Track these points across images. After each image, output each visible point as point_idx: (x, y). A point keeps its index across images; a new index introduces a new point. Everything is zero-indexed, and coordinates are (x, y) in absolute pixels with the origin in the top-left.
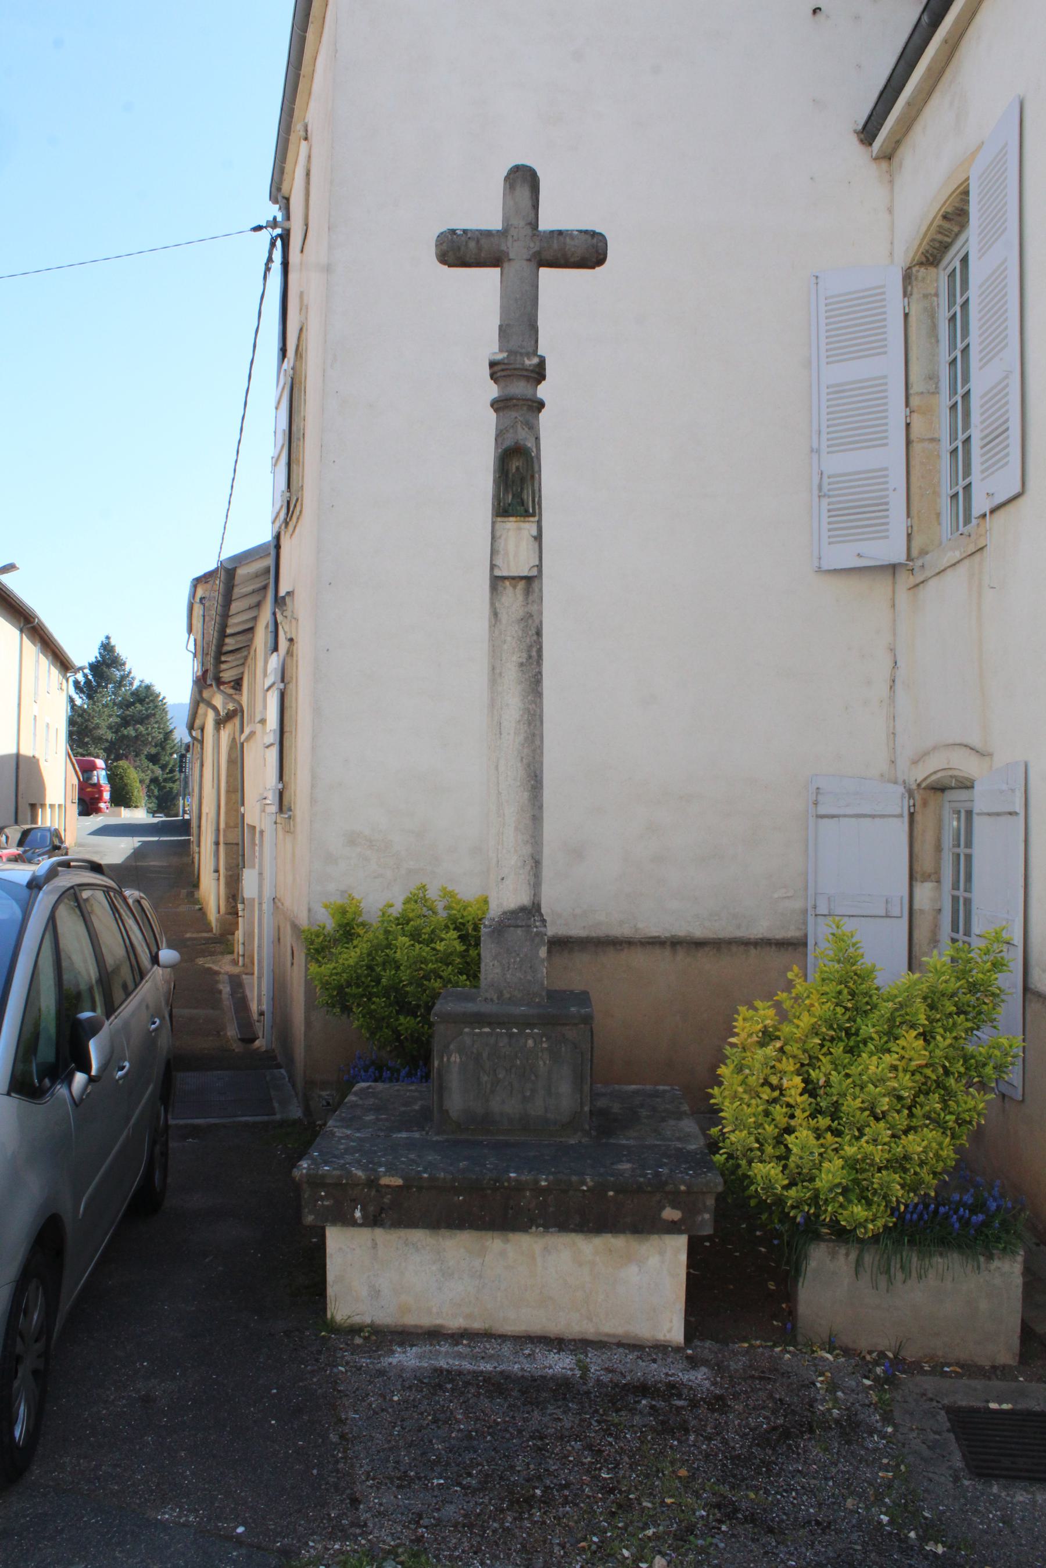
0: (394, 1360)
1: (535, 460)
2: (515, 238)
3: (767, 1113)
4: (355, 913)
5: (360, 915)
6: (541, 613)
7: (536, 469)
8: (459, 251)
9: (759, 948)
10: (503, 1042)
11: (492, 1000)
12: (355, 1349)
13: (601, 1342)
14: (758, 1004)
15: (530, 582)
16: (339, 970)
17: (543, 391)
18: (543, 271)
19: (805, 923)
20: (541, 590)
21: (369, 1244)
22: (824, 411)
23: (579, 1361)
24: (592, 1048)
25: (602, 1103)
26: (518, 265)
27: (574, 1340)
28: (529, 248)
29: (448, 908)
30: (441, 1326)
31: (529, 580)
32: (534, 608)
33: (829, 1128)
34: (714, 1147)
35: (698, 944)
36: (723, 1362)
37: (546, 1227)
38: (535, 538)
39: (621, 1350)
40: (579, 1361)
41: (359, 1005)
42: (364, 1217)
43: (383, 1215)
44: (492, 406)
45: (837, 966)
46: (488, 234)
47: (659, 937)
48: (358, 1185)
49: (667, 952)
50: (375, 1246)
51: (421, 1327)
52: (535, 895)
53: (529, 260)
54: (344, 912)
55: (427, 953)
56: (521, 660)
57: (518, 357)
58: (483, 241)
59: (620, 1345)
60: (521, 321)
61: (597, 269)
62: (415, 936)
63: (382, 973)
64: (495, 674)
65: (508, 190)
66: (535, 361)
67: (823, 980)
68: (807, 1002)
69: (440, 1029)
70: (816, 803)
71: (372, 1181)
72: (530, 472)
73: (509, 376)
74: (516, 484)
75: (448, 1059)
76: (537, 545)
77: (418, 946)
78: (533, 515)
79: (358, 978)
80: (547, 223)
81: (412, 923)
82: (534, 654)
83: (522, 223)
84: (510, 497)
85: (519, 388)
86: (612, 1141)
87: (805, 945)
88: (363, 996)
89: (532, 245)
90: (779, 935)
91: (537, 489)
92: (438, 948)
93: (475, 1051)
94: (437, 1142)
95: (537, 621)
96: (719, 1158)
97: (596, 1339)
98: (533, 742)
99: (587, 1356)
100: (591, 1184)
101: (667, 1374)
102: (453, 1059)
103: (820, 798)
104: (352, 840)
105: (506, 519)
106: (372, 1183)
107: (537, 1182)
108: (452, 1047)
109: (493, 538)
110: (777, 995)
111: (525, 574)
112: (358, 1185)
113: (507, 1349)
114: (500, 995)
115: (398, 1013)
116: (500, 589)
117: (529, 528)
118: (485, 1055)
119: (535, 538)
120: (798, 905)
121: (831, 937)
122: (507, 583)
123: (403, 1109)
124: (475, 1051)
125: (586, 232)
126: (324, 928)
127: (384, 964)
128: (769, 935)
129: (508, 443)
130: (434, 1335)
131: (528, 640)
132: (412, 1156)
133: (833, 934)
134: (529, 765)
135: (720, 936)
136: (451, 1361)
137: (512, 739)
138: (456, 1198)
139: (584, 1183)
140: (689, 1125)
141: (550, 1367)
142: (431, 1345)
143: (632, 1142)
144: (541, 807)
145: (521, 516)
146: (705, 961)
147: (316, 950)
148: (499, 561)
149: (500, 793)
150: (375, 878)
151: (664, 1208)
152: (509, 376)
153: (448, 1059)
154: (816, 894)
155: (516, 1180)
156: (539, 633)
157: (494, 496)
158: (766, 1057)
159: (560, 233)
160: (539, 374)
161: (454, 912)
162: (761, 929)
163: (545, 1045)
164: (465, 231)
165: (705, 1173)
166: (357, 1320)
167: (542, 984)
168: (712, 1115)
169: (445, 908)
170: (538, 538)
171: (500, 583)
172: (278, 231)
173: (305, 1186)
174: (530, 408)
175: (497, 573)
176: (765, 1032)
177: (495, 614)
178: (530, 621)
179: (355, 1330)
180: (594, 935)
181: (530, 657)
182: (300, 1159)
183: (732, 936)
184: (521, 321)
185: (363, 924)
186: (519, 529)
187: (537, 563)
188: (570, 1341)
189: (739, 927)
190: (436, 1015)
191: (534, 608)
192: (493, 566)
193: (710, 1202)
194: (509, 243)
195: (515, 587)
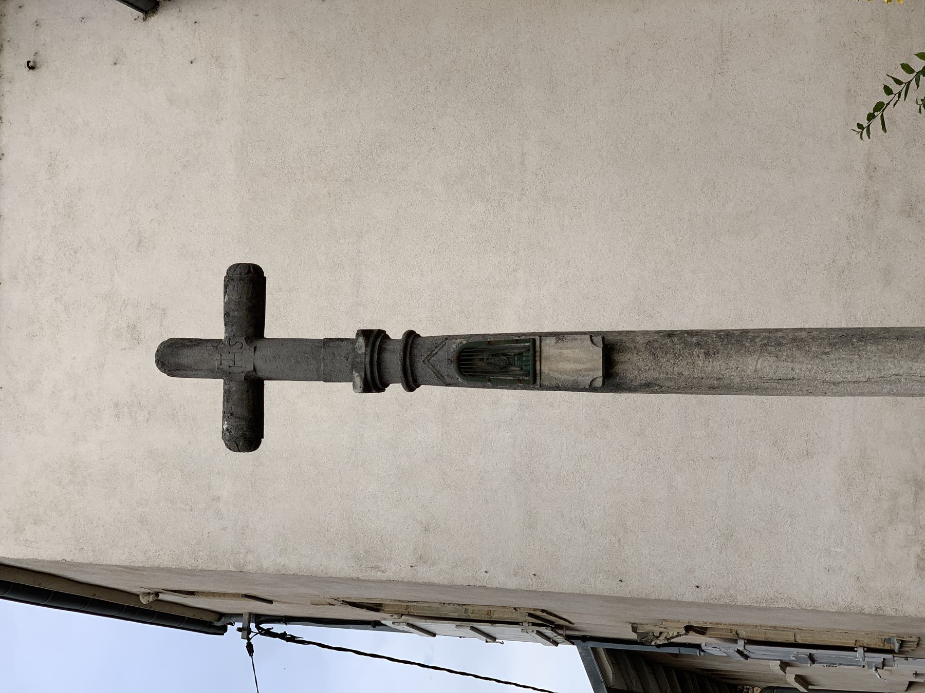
1: (471, 340)
2: (231, 364)
6: (646, 333)
7: (481, 339)
8: (246, 428)
17: (396, 333)
18: (268, 334)
32: (640, 340)
46: (227, 394)
56: (702, 356)
66: (361, 340)
78: (534, 340)
80: (216, 330)
82: (694, 339)
84: (513, 368)
98: (802, 340)
109: (558, 388)
125: (226, 287)
129: (452, 370)
149: (869, 380)
156: (670, 334)
159: (227, 314)
160: (375, 338)
177: (648, 387)
178: (656, 345)
181: (698, 344)
186: (547, 358)
191: (640, 340)
192: (592, 388)
194: (236, 370)
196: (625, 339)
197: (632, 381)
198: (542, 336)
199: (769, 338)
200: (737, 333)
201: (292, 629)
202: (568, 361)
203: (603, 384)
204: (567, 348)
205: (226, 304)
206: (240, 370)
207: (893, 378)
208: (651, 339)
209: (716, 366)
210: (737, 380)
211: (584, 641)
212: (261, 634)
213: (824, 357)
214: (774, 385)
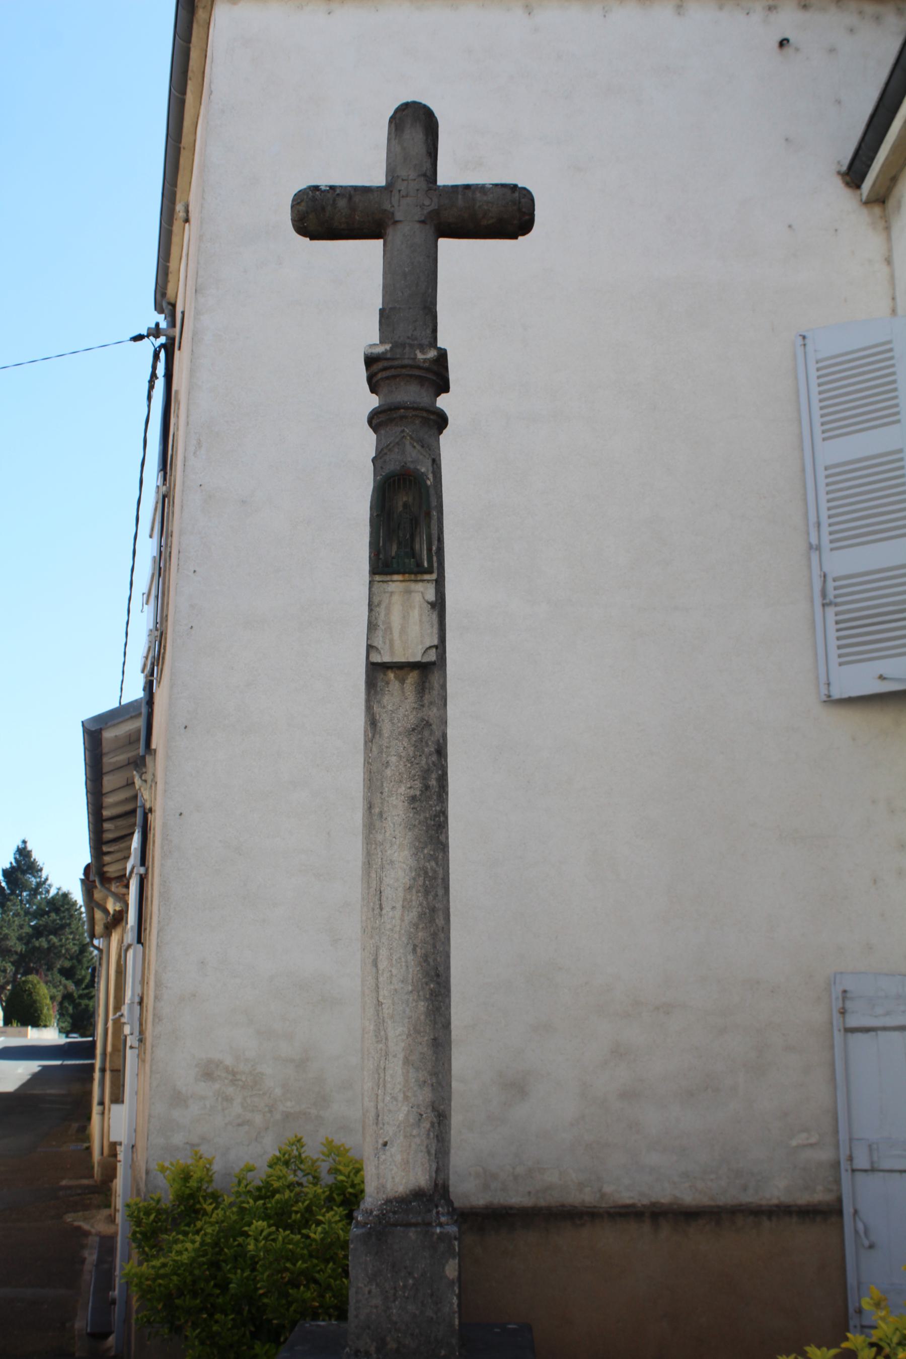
1: (432, 491)
4: (201, 1180)
5: (211, 1181)
7: (434, 503)
8: (324, 215)
15: (428, 672)
16: (167, 1270)
18: (443, 242)
19: (838, 1181)
20: (444, 687)
22: (823, 497)
26: (407, 230)
28: (422, 206)
29: (334, 1171)
32: (433, 713)
38: (433, 605)
41: (195, 1326)
44: (370, 422)
47: (633, 1206)
52: (437, 1171)
53: (423, 222)
55: (297, 1244)
56: (412, 792)
57: (407, 349)
58: (357, 199)
60: (411, 305)
61: (520, 238)
62: (280, 1218)
63: (231, 1276)
64: (373, 815)
65: (393, 135)
66: (432, 354)
70: (843, 1012)
73: (394, 377)
74: (406, 527)
76: (435, 617)
77: (282, 1234)
78: (431, 572)
79: (194, 1282)
80: (448, 174)
81: (277, 1196)
82: (433, 782)
83: (413, 175)
85: (410, 394)
87: (840, 1212)
89: (427, 202)
90: (803, 1199)
91: (435, 532)
92: (312, 1235)
95: (438, 734)
98: (432, 920)
103: (849, 1005)
104: (208, 1072)
105: (388, 578)
110: (847, 1339)
111: (418, 658)
119: (433, 605)
120: (825, 1155)
122: (391, 675)
126: (158, 1201)
127: (235, 1258)
128: (786, 1199)
134: (426, 958)
135: (721, 1203)
137: (398, 918)
144: (447, 1026)
145: (410, 573)
148: (378, 642)
149: (380, 1004)
150: (239, 1125)
152: (394, 377)
154: (851, 1140)
156: (441, 751)
157: (370, 543)
159: (467, 187)
161: (341, 1178)
164: (332, 188)
169: (331, 1171)
170: (439, 605)
171: (381, 676)
172: (162, 340)
174: (425, 422)
175: (376, 658)
177: (373, 723)
178: (426, 733)
180: (542, 1203)
181: (427, 787)
184: (411, 305)
185: (215, 1197)
186: (409, 592)
187: (436, 642)
189: (745, 1188)
191: (434, 712)
192: (370, 648)
195: (402, 681)
196: (435, 693)
197: (379, 702)
198: (440, 584)
199: (435, 878)
200: (442, 838)
201: (160, 384)
202: (404, 617)
204: (421, 615)
205: (481, 188)
206: (396, 205)
207: (382, 1033)
208: (434, 727)
209: (397, 810)
210: (380, 838)
212: (155, 350)
213: (410, 947)
214: (374, 884)
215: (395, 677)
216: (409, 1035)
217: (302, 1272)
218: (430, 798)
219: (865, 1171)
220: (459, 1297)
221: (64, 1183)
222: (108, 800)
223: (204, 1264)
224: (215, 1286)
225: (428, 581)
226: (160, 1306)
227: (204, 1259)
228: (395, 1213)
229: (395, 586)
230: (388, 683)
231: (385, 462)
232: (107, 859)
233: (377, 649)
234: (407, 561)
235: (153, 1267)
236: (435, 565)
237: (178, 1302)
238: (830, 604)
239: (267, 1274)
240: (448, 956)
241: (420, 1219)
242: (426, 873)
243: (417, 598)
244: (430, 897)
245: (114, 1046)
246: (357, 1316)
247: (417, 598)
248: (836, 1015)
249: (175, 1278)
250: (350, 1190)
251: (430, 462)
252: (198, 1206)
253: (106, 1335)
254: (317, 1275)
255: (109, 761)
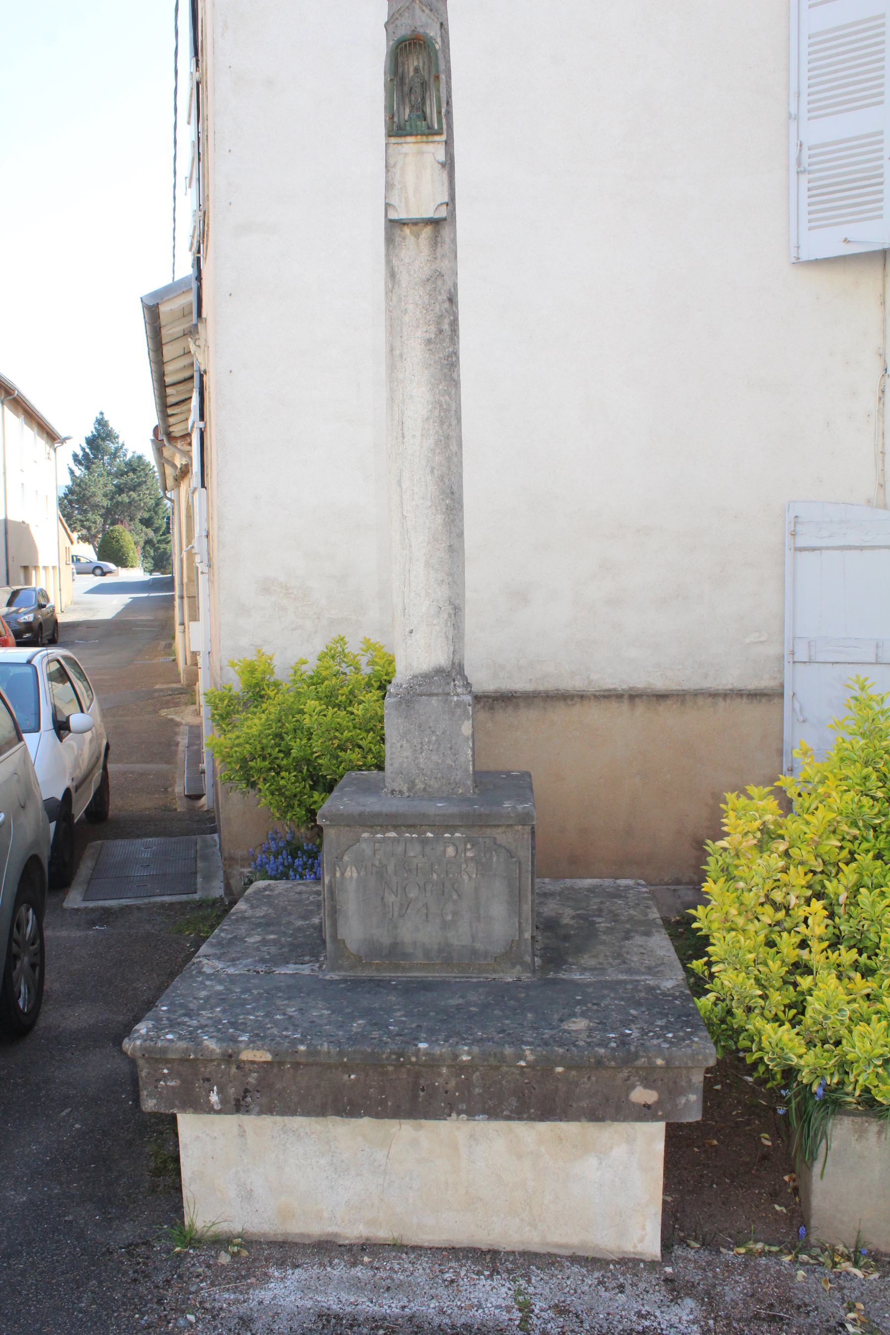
0: (265, 1295)
1: (440, 55)
3: (771, 944)
4: (264, 672)
7: (442, 67)
9: (728, 701)
10: (414, 851)
11: (401, 792)
12: (219, 1276)
13: (549, 1255)
14: (752, 790)
16: (241, 740)
19: (781, 671)
20: (454, 241)
21: (235, 1130)
23: (519, 1292)
24: (533, 855)
25: (550, 908)
27: (513, 1252)
30: (336, 1235)
31: (435, 223)
32: (444, 265)
33: (856, 966)
34: (699, 985)
35: (661, 697)
36: (714, 1286)
37: (471, 1114)
38: (443, 165)
39: (575, 1269)
40: (519, 1292)
42: (223, 1101)
43: (249, 1099)
45: (862, 742)
47: (615, 690)
48: (212, 1061)
49: (625, 706)
50: (242, 1134)
51: (309, 1236)
52: (454, 651)
54: (253, 671)
55: (343, 718)
56: (428, 336)
59: (575, 1259)
62: (330, 699)
63: (292, 743)
64: (394, 357)
67: (842, 760)
68: (821, 790)
69: (330, 835)
70: (794, 534)
71: (230, 1056)
72: (433, 72)
75: (343, 874)
77: (331, 710)
78: (439, 133)
79: (263, 749)
81: (326, 682)
82: (446, 327)
86: (561, 975)
87: (781, 695)
88: (270, 769)
90: (752, 684)
92: (355, 711)
93: (377, 863)
94: (332, 982)
95: (450, 284)
96: (705, 1003)
97: (542, 1250)
98: (447, 446)
99: (529, 1282)
100: (531, 1057)
101: (639, 1315)
102: (348, 874)
103: (799, 528)
104: (266, 587)
105: (402, 140)
106: (229, 1058)
107: (456, 1056)
108: (346, 858)
110: (779, 780)
111: (430, 214)
112: (212, 1061)
113: (422, 1271)
114: (412, 785)
115: (312, 788)
116: (397, 239)
117: (435, 151)
118: (391, 868)
119: (443, 165)
121: (853, 703)
122: (407, 231)
123: (300, 923)
124: (377, 863)
126: (230, 690)
127: (295, 730)
128: (739, 685)
129: (403, 31)
130: (326, 1248)
131: (437, 309)
132: (291, 1011)
133: (856, 699)
134: (442, 478)
135: (686, 688)
136: (344, 1296)
137: (419, 444)
138: (346, 1077)
139: (522, 1057)
140: (661, 945)
141: (480, 1306)
142: (322, 1265)
143: (587, 977)
144: (461, 535)
145: (423, 135)
146: (668, 717)
147: (221, 716)
148: (394, 201)
150: (293, 629)
151: (633, 1087)
153: (343, 874)
154: (794, 638)
155: (427, 1054)
156: (452, 300)
157: (385, 107)
158: (768, 868)
162: (730, 680)
163: (470, 854)
165: (689, 1036)
166: (224, 1227)
167: (467, 770)
168: (692, 943)
169: (368, 664)
170: (449, 165)
171: (397, 231)
173: (141, 1062)
175: (393, 216)
176: (764, 829)
177: (392, 275)
178: (439, 283)
179: (221, 1242)
182: (137, 1020)
183: (698, 687)
185: (277, 685)
186: (421, 153)
187: (446, 199)
188: (508, 1253)
190: (323, 816)
192: (387, 205)
193: (698, 1078)
195: (417, 236)
196: (446, 246)
198: (449, 144)
199: (449, 411)
200: (455, 376)
203: (391, 221)
207: (407, 541)
208: (446, 277)
209: (415, 352)
210: (401, 376)
211: (196, 279)
213: (428, 470)
215: (411, 233)
216: (429, 543)
217: (347, 740)
218: (443, 340)
219: (805, 662)
220: (473, 750)
221: (157, 687)
222: (168, 368)
223: (269, 735)
224: (280, 751)
225: (439, 142)
226: (238, 768)
227: (270, 732)
228: (420, 685)
229: (409, 146)
230: (404, 238)
231: (396, 26)
232: (172, 420)
233: (394, 207)
234: (419, 123)
235: (230, 739)
236: (445, 126)
237: (251, 764)
238: (804, 172)
239: (320, 741)
240: (461, 477)
241: (440, 691)
242: (441, 406)
243: (428, 159)
244: (445, 427)
245: (188, 577)
246: (392, 765)
247: (428, 159)
248: (788, 537)
249: (247, 746)
250: (385, 677)
251: (438, 25)
252: (263, 693)
253: (199, 797)
254: (361, 742)
255: (167, 333)
